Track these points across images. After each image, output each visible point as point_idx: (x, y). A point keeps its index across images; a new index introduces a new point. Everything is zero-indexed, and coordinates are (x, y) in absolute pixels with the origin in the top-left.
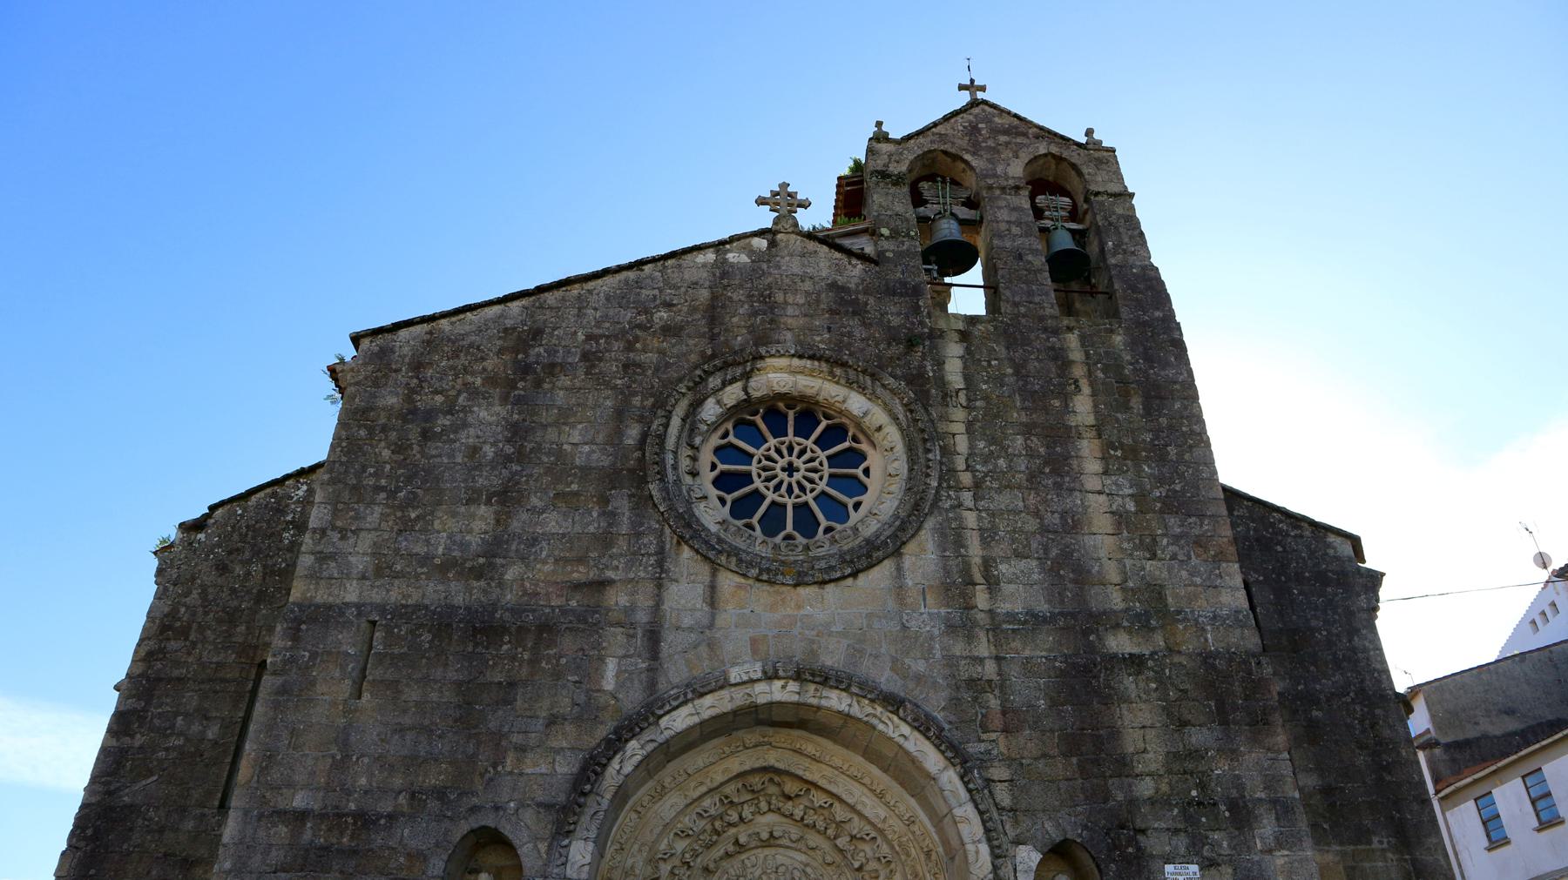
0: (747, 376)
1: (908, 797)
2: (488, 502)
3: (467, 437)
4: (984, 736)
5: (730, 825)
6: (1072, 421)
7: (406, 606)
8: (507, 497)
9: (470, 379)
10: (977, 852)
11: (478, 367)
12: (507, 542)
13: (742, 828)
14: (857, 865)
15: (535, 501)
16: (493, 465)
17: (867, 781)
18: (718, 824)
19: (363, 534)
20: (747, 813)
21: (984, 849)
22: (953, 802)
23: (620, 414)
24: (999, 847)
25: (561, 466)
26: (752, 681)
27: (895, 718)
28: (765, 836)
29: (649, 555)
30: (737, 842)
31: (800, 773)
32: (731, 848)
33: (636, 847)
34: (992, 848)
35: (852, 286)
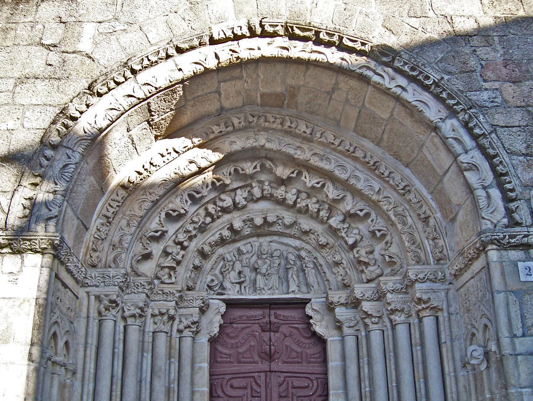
1: (402, 167)
4: (486, 85)
5: (225, 210)
10: (489, 197)
13: (236, 214)
14: (351, 241)
17: (359, 154)
18: (211, 208)
20: (241, 197)
21: (495, 193)
22: (458, 149)
24: (512, 190)
26: (237, 38)
27: (390, 70)
28: (259, 221)
30: (231, 228)
31: (291, 151)
32: (226, 233)
33: (124, 222)
34: (504, 192)
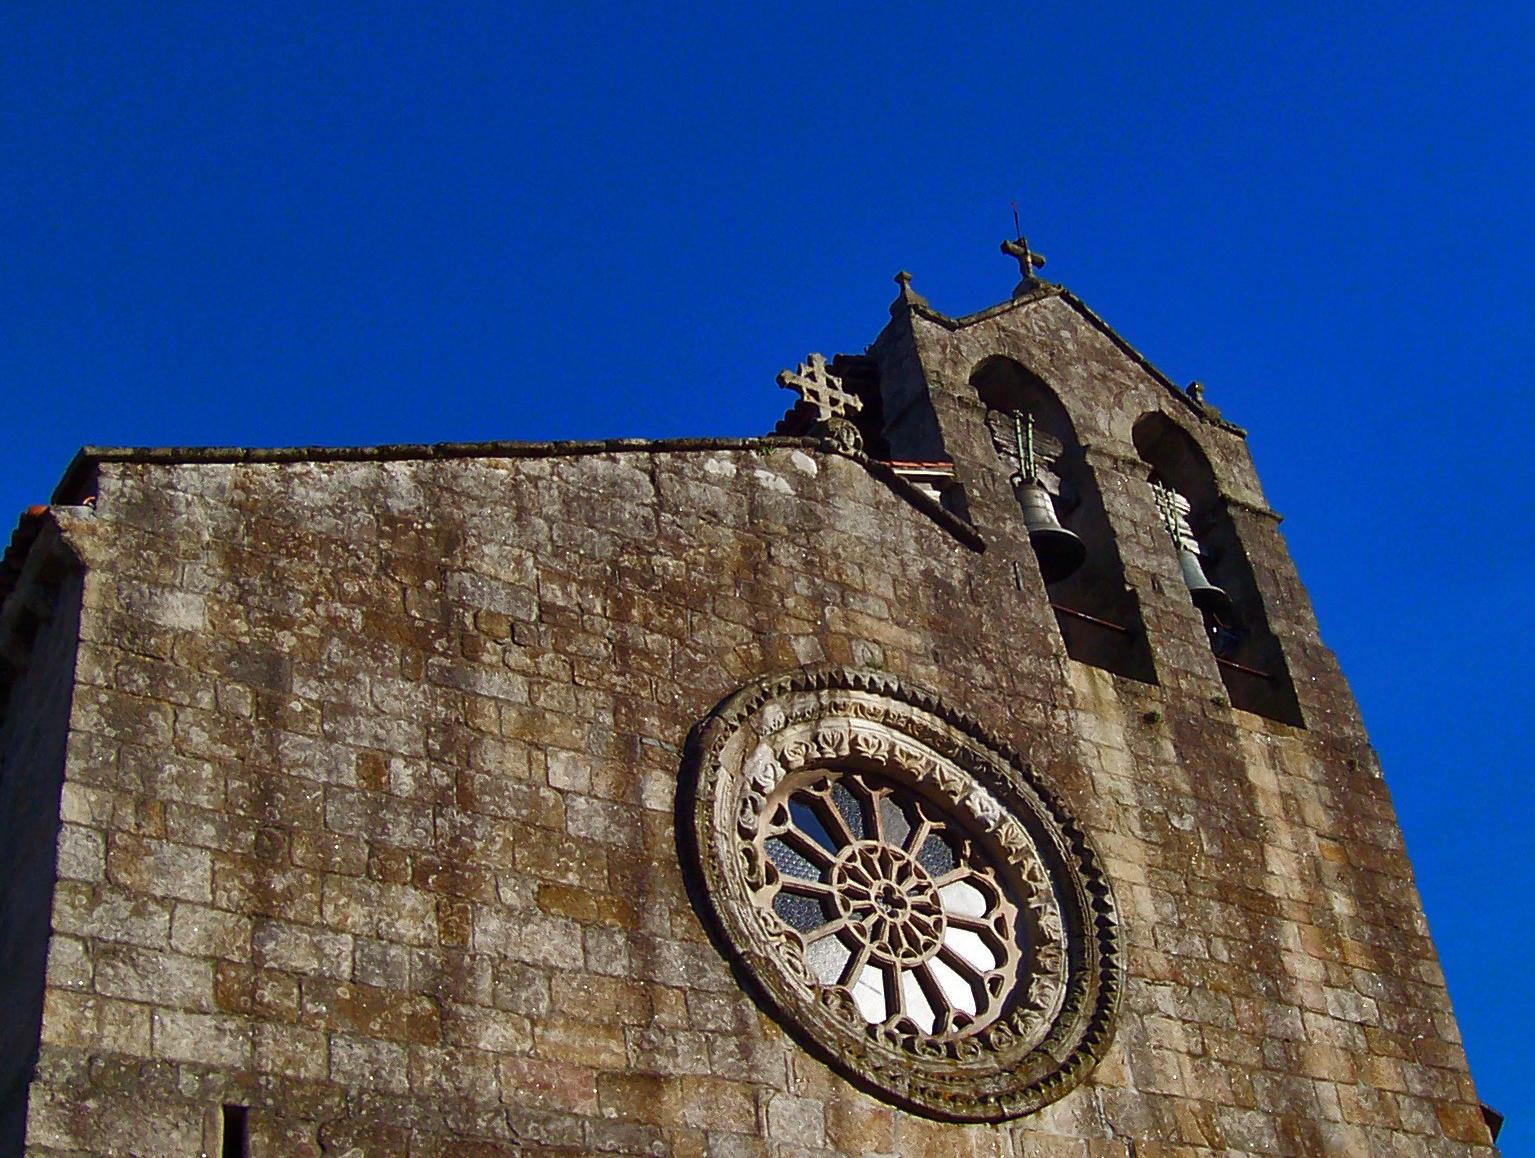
0: (820, 713)
2: (419, 880)
3: (360, 733)
6: (1276, 888)
7: (298, 1082)
8: (452, 882)
9: (342, 611)
11: (351, 587)
12: (471, 972)
15: (509, 896)
16: (417, 806)
19: (180, 910)
23: (629, 752)
25: (539, 831)
29: (725, 1034)
35: (955, 583)
